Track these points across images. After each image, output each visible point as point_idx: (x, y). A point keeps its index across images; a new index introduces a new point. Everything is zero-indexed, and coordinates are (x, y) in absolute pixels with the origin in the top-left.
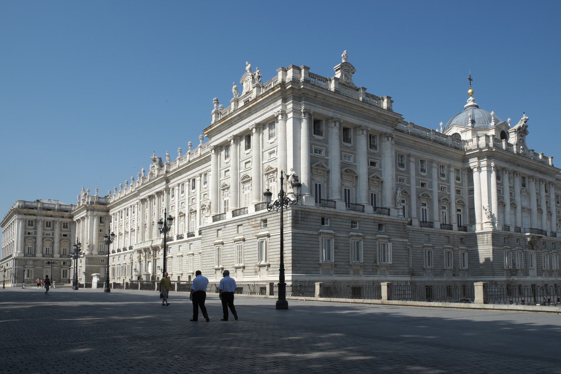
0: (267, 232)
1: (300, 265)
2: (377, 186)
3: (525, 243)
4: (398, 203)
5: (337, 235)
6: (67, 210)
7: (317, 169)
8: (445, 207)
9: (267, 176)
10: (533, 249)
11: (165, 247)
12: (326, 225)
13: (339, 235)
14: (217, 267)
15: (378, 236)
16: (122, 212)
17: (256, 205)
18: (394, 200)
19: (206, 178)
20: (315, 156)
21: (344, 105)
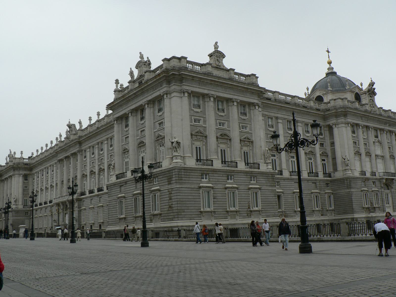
0: (158, 188)
1: (185, 213)
2: (249, 145)
3: (381, 185)
4: (266, 158)
8: (311, 158)
9: (157, 142)
10: (388, 189)
12: (204, 180)
13: (216, 188)
16: (43, 170)
18: (263, 157)
19: (112, 142)
20: (194, 125)
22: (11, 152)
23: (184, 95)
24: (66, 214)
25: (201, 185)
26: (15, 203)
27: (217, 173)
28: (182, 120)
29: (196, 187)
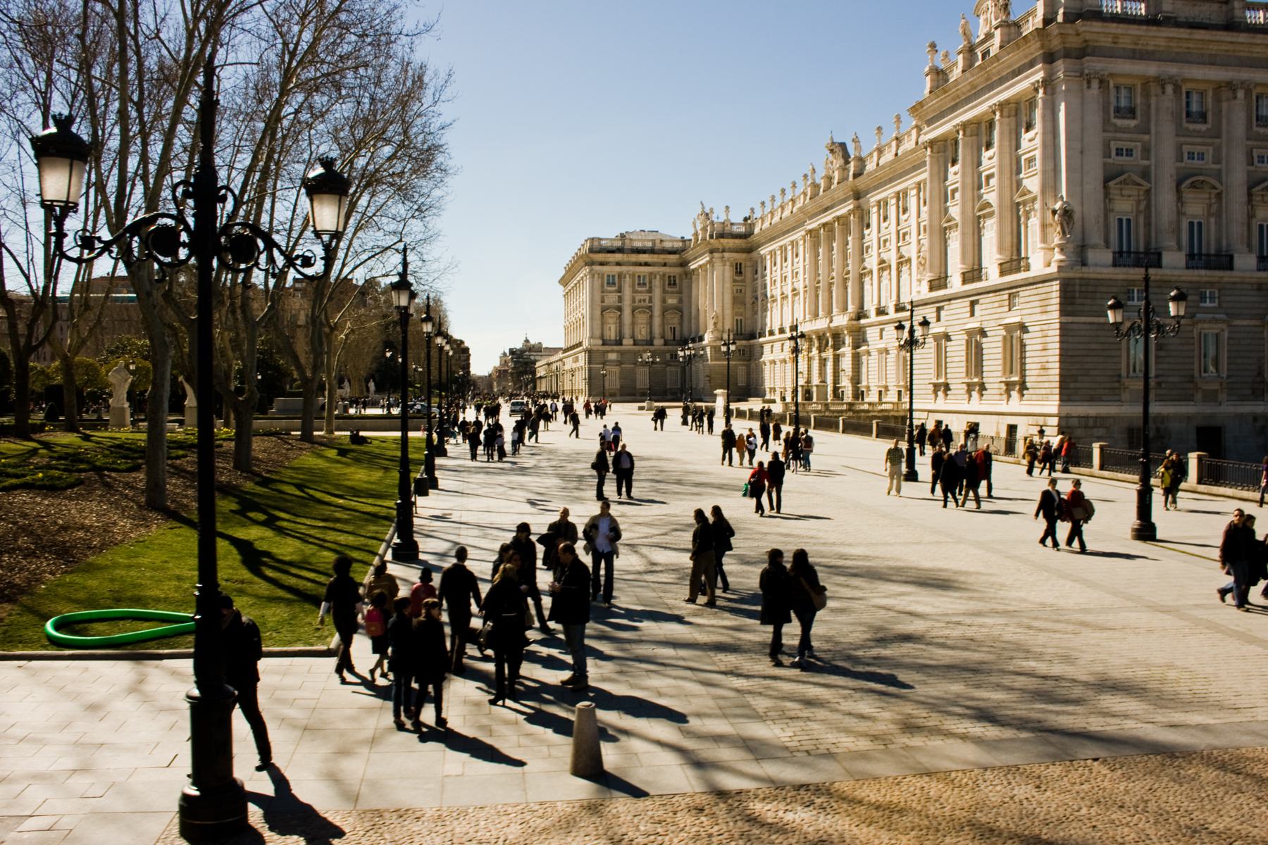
1: (1079, 385)
7: (1121, 189)
14: (935, 381)
17: (1001, 264)
21: (1185, 45)
22: (703, 208)
23: (1089, 87)
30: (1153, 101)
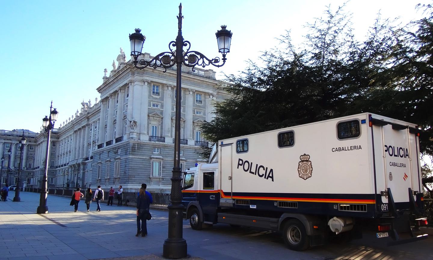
1: (135, 179)
5: (164, 159)
6: (34, 136)
11: (84, 164)
13: (166, 159)
15: (198, 160)
20: (153, 108)
24: (76, 174)
25: (152, 156)
26: (43, 164)
27: (168, 147)
28: (141, 104)
29: (147, 158)
30: (165, 91)
